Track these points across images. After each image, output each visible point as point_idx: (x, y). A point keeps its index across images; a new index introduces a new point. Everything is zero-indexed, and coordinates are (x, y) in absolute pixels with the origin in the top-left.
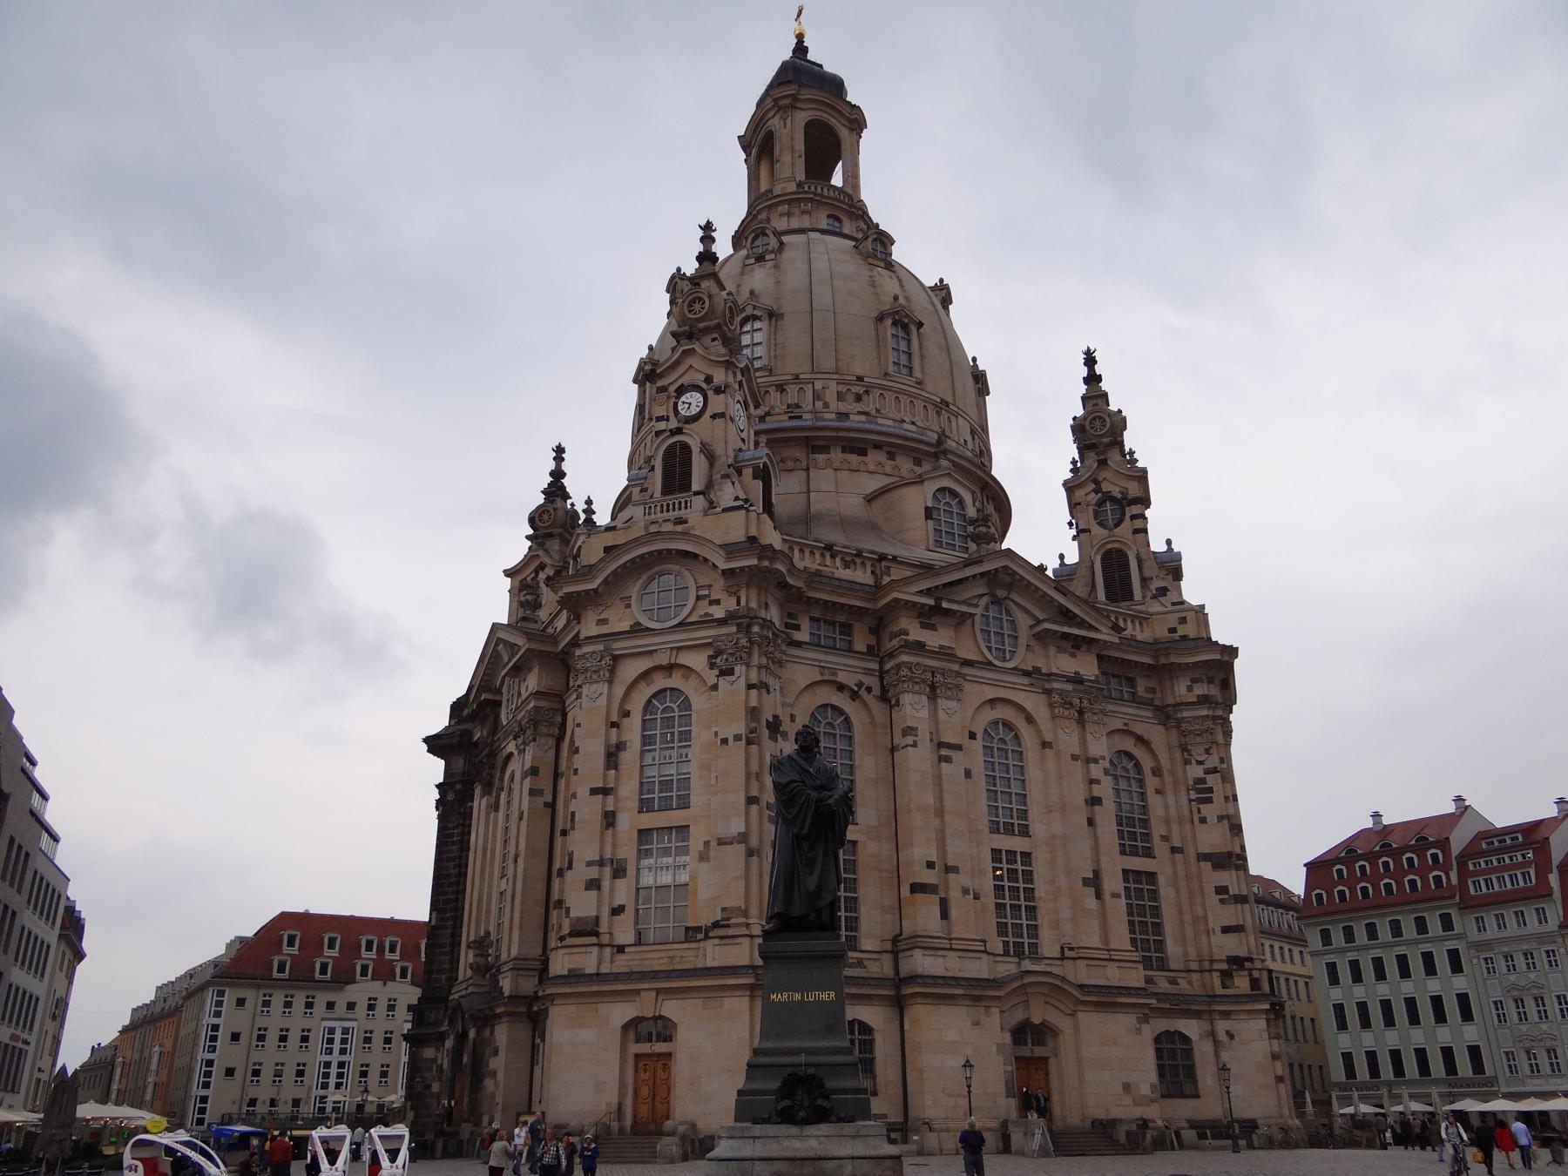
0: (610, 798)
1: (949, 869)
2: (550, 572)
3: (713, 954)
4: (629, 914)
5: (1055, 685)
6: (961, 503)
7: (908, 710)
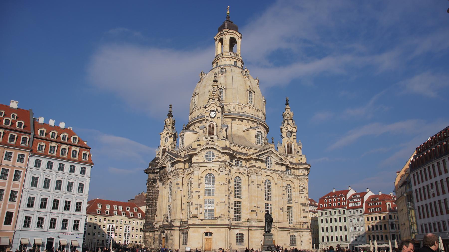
1: (258, 207)
2: (170, 135)
4: (203, 214)
6: (262, 134)
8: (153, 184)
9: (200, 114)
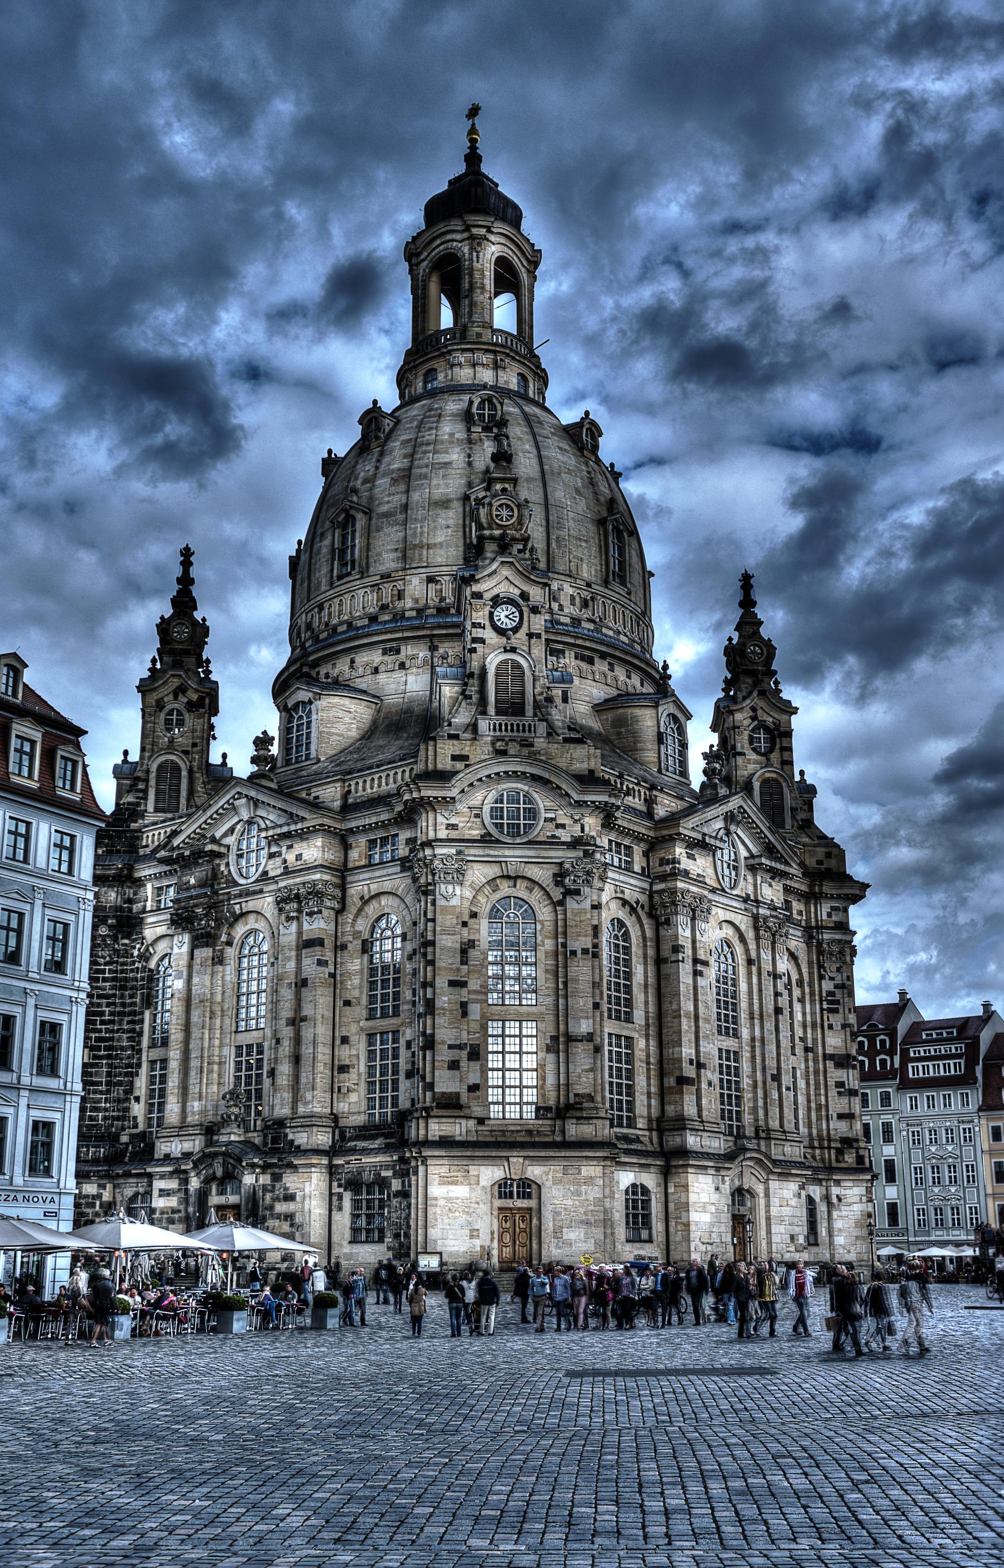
0: (464, 991)
2: (194, 697)
3: (574, 1130)
5: (761, 911)
7: (680, 930)
8: (115, 939)
9: (384, 607)
